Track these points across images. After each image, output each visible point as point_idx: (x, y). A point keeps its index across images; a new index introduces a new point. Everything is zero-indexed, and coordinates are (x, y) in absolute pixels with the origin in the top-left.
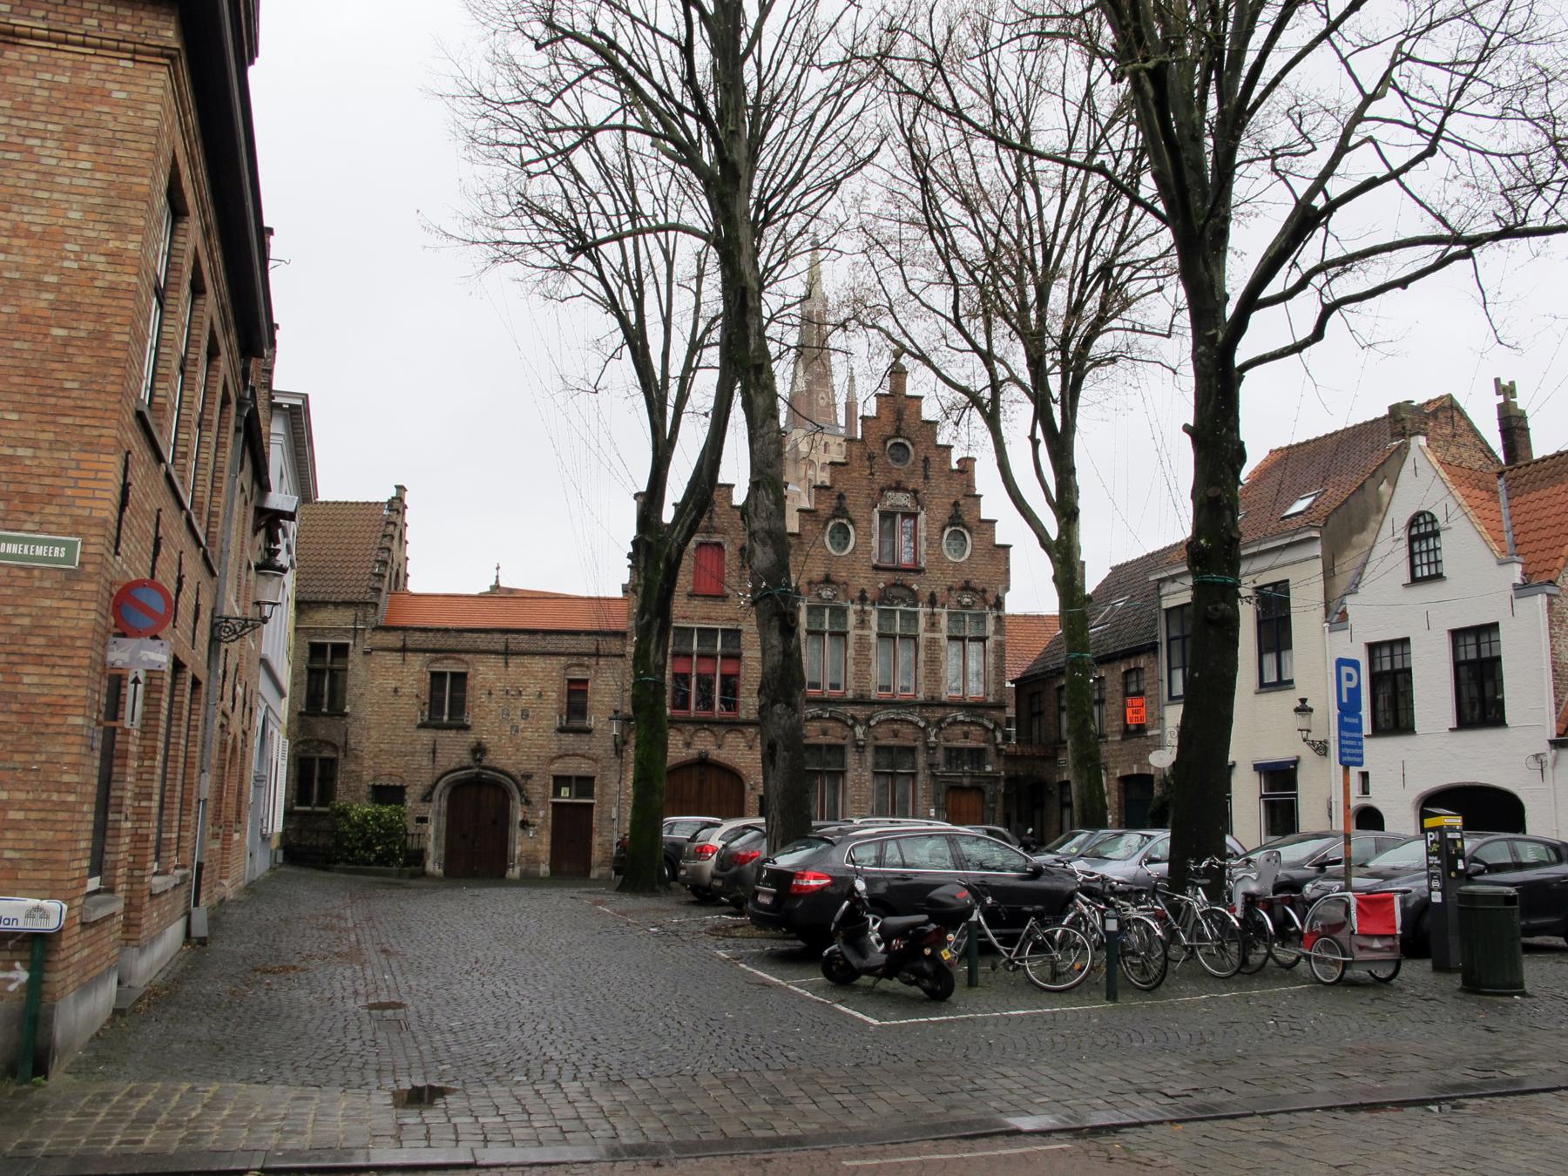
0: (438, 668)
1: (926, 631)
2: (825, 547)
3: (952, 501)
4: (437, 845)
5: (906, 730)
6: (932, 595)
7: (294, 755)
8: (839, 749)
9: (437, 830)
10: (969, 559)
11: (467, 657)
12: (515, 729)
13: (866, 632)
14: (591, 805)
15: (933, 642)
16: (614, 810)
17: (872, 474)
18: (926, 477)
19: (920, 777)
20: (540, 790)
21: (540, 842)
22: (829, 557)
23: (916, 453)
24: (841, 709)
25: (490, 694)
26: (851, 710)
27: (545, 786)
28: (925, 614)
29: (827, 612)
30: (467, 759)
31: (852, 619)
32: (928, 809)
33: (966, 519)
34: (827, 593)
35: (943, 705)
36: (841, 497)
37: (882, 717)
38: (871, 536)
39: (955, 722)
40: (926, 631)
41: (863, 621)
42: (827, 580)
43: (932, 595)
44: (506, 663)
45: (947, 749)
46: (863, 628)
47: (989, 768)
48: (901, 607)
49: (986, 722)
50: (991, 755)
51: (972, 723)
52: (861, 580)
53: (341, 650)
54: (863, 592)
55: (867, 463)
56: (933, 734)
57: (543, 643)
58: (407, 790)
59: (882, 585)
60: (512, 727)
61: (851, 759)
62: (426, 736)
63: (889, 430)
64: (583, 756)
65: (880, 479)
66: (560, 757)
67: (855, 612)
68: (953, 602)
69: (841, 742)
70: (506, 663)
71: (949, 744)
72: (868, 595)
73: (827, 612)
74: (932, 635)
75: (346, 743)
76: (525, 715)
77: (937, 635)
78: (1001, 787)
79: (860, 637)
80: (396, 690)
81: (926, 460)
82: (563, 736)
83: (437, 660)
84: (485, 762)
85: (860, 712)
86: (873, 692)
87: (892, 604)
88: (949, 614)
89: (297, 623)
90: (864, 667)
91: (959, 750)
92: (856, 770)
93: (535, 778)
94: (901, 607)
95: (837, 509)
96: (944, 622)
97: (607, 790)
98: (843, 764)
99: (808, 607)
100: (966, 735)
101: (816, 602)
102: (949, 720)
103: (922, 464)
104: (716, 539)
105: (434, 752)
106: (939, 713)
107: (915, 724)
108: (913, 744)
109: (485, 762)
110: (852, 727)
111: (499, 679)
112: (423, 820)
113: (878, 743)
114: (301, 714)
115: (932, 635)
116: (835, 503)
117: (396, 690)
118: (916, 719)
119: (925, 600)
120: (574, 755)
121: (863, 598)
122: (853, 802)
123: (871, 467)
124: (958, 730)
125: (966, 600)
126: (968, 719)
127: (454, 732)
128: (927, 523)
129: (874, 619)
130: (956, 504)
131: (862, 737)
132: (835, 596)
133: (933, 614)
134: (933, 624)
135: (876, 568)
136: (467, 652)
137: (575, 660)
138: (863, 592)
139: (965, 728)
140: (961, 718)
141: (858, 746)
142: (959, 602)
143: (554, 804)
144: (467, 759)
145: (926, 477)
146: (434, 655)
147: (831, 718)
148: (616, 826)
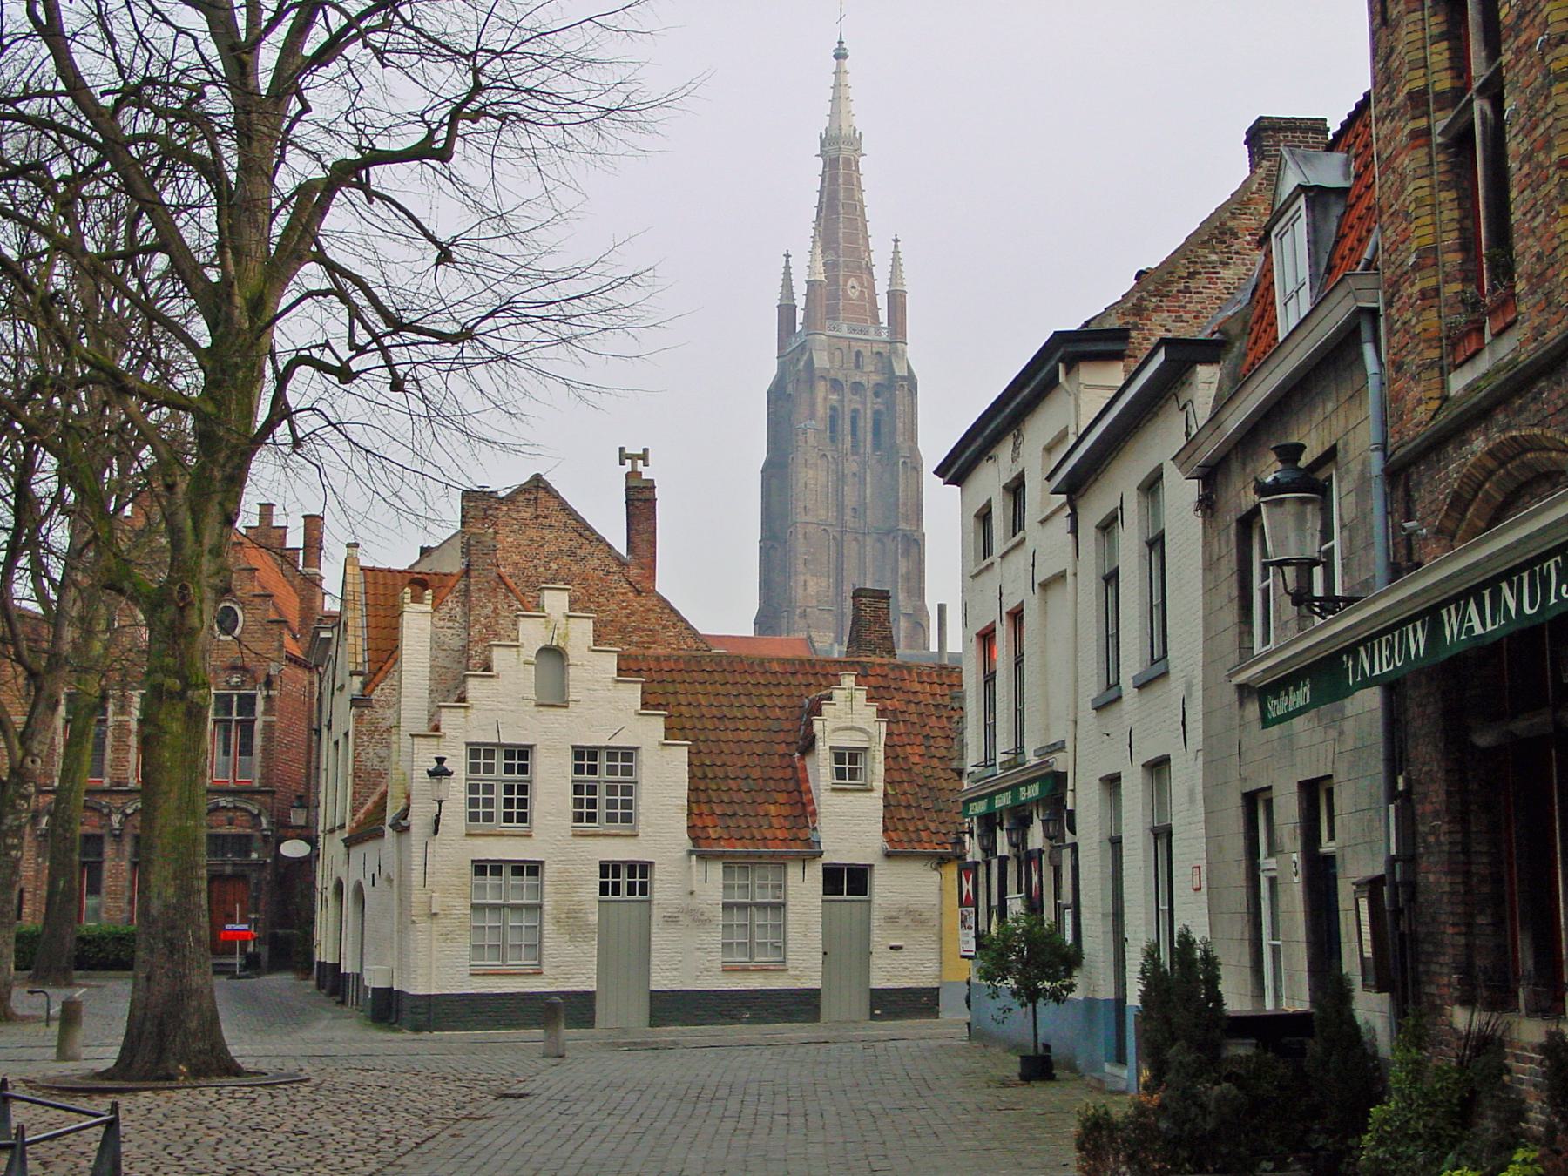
8: (100, 838)
24: (97, 798)
26: (106, 800)
46: (122, 714)
47: (254, 856)
50: (257, 844)
61: (109, 849)
69: (99, 831)
78: (267, 875)
86: (131, 779)
91: (224, 837)
92: (113, 860)
98: (100, 854)
110: (109, 815)
122: (109, 893)
124: (222, 816)
125: (235, 680)
126: (230, 805)
139: (231, 814)
140: (223, 804)
141: (115, 836)
142: (227, 682)
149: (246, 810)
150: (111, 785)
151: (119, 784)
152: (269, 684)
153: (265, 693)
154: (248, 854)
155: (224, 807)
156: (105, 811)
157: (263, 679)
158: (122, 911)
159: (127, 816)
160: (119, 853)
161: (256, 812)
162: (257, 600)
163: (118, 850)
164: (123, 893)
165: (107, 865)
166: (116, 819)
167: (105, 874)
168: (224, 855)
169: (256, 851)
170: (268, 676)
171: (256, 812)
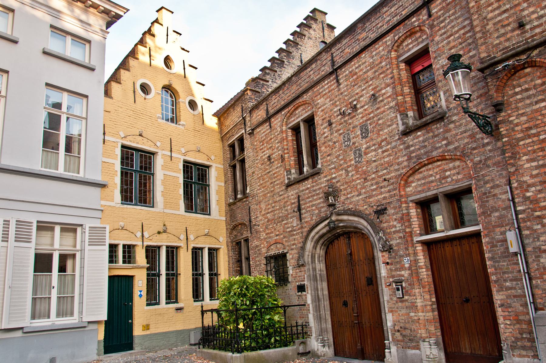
0: (294, 121)
4: (319, 318)
7: (232, 242)
9: (317, 299)
11: (305, 97)
12: (359, 154)
14: (477, 235)
16: (511, 236)
20: (399, 226)
21: (413, 307)
25: (330, 124)
27: (405, 219)
30: (325, 210)
44: (338, 81)
53: (241, 140)
57: (364, 35)
58: (289, 256)
60: (355, 153)
62: (292, 193)
64: (443, 158)
66: (415, 171)
70: (338, 81)
75: (250, 221)
76: (365, 133)
80: (269, 158)
82: (409, 140)
83: (292, 114)
84: (339, 207)
89: (221, 134)
93: (391, 211)
97: (491, 202)
105: (299, 209)
109: (339, 207)
111: (334, 104)
112: (301, 288)
114: (230, 205)
117: (269, 158)
120: (431, 161)
127: (310, 180)
136: (306, 91)
137: (402, 31)
143: (427, 244)
144: (325, 210)
146: (286, 110)
148: (522, 267)
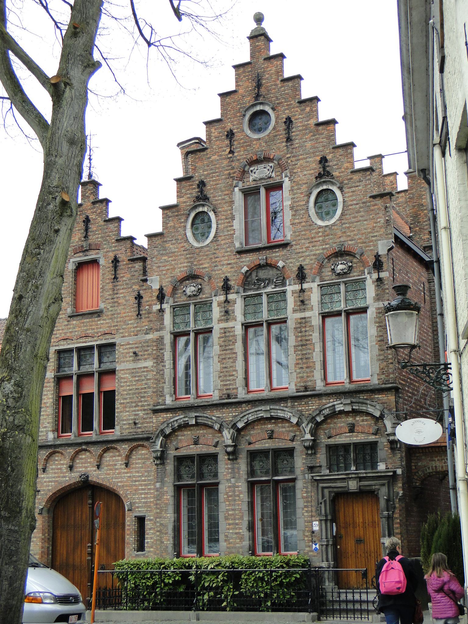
1: (294, 311)
2: (187, 241)
3: (318, 158)
5: (280, 429)
6: (301, 269)
10: (340, 219)
13: (230, 324)
15: (303, 322)
17: (231, 152)
18: (289, 139)
19: (299, 484)
22: (192, 252)
23: (277, 118)
24: (208, 413)
26: (217, 414)
28: (293, 292)
29: (192, 308)
31: (216, 312)
32: (312, 522)
33: (336, 174)
34: (190, 289)
35: (319, 396)
36: (202, 184)
37: (251, 418)
38: (233, 218)
39: (334, 414)
40: (294, 311)
41: (227, 312)
42: (192, 277)
43: (301, 269)
45: (330, 448)
46: (227, 320)
47: (382, 467)
48: (269, 289)
49: (371, 410)
51: (355, 412)
52: (224, 268)
54: (226, 280)
55: (227, 142)
56: (307, 430)
59: (245, 269)
63: (249, 100)
65: (242, 155)
67: (219, 305)
68: (327, 273)
69: (212, 450)
71: (332, 441)
72: (231, 283)
73: (192, 308)
74: (302, 315)
77: (307, 314)
79: (225, 331)
81: (289, 121)
85: (228, 415)
87: (258, 289)
88: (321, 287)
90: (229, 363)
91: (346, 447)
92: (228, 480)
94: (269, 289)
95: (198, 198)
96: (315, 297)
99: (174, 308)
100: (352, 429)
101: (182, 300)
102: (326, 412)
103: (283, 126)
104: (92, 255)
106: (313, 406)
107: (288, 421)
108: (290, 445)
110: (220, 431)
113: (252, 447)
115: (302, 315)
116: (195, 192)
118: (287, 415)
119: (294, 275)
121: (226, 288)
123: (231, 145)
124: (342, 423)
125: (340, 267)
126: (348, 408)
128: (292, 190)
129: (238, 308)
130: (324, 160)
131: (230, 442)
132: (200, 290)
133: (302, 291)
134: (302, 302)
135: (240, 252)
138: (226, 280)
139: (350, 420)
140: (339, 408)
141: (228, 454)
145: (289, 139)
147: (197, 424)
149: (368, 414)
150: (221, 398)
151: (229, 396)
152: (378, 265)
153: (375, 276)
154: (374, 465)
155: (341, 412)
156: (217, 427)
157: (371, 261)
158: (242, 539)
159: (239, 431)
160: (234, 472)
161: (377, 414)
162: (356, 177)
163: (233, 469)
164: (242, 518)
165: (222, 488)
166: (227, 435)
167: (222, 497)
168: (347, 468)
169: (383, 460)
170: (377, 257)
171: (377, 414)
